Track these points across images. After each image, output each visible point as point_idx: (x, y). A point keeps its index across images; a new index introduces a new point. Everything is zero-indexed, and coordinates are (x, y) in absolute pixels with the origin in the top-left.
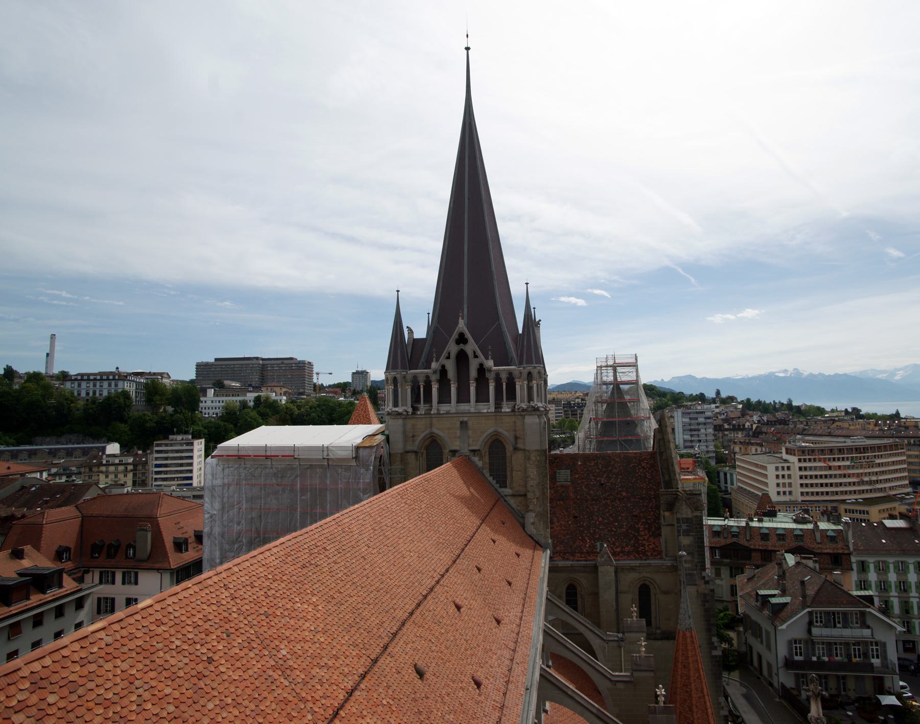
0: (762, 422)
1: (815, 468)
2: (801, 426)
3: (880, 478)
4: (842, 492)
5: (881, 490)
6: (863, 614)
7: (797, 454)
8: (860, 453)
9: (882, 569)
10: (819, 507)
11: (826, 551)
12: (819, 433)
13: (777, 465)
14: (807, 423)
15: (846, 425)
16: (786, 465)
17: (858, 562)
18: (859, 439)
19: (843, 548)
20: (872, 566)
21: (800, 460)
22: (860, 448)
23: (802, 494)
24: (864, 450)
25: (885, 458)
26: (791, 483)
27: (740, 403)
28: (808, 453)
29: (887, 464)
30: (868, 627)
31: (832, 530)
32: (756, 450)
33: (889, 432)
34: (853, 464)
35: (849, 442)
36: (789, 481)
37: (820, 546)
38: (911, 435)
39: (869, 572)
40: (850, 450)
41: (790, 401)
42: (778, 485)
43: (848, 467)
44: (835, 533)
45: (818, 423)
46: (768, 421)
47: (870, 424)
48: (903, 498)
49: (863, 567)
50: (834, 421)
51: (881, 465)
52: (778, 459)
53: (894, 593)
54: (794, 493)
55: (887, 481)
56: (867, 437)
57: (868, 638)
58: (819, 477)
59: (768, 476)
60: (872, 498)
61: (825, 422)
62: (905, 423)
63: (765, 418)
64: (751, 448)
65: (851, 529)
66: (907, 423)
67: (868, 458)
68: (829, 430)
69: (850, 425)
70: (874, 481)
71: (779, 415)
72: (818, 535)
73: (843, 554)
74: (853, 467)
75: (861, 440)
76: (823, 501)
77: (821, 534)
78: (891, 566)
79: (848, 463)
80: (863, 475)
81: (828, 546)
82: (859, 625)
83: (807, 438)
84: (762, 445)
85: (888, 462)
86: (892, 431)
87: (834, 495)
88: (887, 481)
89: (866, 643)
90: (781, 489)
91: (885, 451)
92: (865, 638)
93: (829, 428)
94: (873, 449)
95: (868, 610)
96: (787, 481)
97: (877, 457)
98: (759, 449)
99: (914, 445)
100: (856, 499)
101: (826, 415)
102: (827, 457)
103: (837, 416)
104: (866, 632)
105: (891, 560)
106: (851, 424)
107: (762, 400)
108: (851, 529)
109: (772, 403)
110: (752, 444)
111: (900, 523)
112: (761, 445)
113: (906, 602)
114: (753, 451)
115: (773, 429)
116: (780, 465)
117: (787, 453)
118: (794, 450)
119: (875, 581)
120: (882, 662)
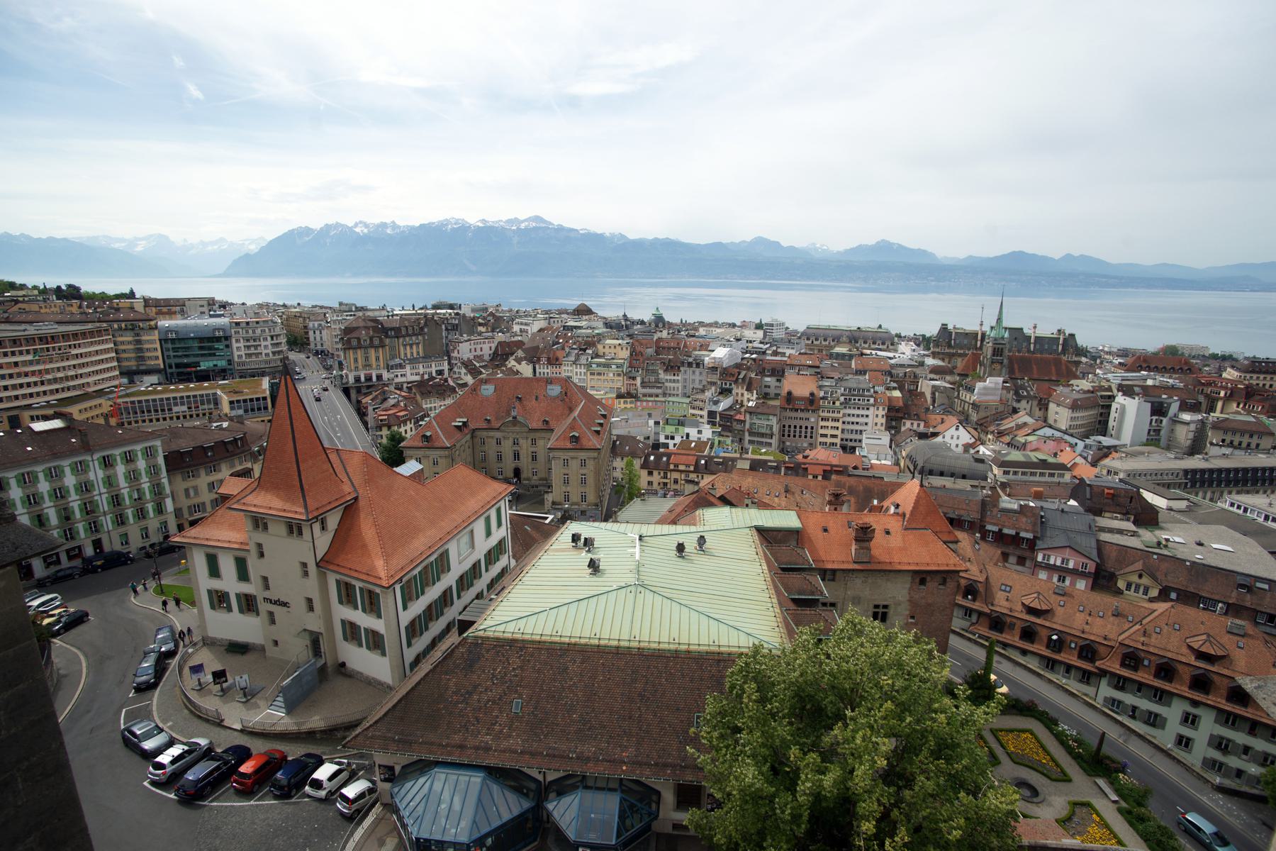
3: (80, 371)
4: (24, 396)
5: (74, 387)
8: (47, 344)
15: (35, 307)
22: (46, 337)
33: (94, 315)
34: (37, 358)
35: (31, 330)
38: (121, 319)
39: (10, 488)
40: (30, 340)
43: (31, 363)
48: (112, 392)
50: (17, 302)
51: (79, 356)
55: (89, 374)
56: (58, 323)
60: (71, 397)
67: (60, 349)
74: (38, 362)
75: (51, 327)
79: (30, 357)
86: (98, 315)
88: (89, 374)
91: (83, 339)
93: (5, 312)
94: (66, 338)
97: (73, 346)
99: (126, 329)
100: (48, 402)
102: (24, 348)
103: (24, 296)
105: (39, 469)
106: (43, 306)
119: (21, 498)
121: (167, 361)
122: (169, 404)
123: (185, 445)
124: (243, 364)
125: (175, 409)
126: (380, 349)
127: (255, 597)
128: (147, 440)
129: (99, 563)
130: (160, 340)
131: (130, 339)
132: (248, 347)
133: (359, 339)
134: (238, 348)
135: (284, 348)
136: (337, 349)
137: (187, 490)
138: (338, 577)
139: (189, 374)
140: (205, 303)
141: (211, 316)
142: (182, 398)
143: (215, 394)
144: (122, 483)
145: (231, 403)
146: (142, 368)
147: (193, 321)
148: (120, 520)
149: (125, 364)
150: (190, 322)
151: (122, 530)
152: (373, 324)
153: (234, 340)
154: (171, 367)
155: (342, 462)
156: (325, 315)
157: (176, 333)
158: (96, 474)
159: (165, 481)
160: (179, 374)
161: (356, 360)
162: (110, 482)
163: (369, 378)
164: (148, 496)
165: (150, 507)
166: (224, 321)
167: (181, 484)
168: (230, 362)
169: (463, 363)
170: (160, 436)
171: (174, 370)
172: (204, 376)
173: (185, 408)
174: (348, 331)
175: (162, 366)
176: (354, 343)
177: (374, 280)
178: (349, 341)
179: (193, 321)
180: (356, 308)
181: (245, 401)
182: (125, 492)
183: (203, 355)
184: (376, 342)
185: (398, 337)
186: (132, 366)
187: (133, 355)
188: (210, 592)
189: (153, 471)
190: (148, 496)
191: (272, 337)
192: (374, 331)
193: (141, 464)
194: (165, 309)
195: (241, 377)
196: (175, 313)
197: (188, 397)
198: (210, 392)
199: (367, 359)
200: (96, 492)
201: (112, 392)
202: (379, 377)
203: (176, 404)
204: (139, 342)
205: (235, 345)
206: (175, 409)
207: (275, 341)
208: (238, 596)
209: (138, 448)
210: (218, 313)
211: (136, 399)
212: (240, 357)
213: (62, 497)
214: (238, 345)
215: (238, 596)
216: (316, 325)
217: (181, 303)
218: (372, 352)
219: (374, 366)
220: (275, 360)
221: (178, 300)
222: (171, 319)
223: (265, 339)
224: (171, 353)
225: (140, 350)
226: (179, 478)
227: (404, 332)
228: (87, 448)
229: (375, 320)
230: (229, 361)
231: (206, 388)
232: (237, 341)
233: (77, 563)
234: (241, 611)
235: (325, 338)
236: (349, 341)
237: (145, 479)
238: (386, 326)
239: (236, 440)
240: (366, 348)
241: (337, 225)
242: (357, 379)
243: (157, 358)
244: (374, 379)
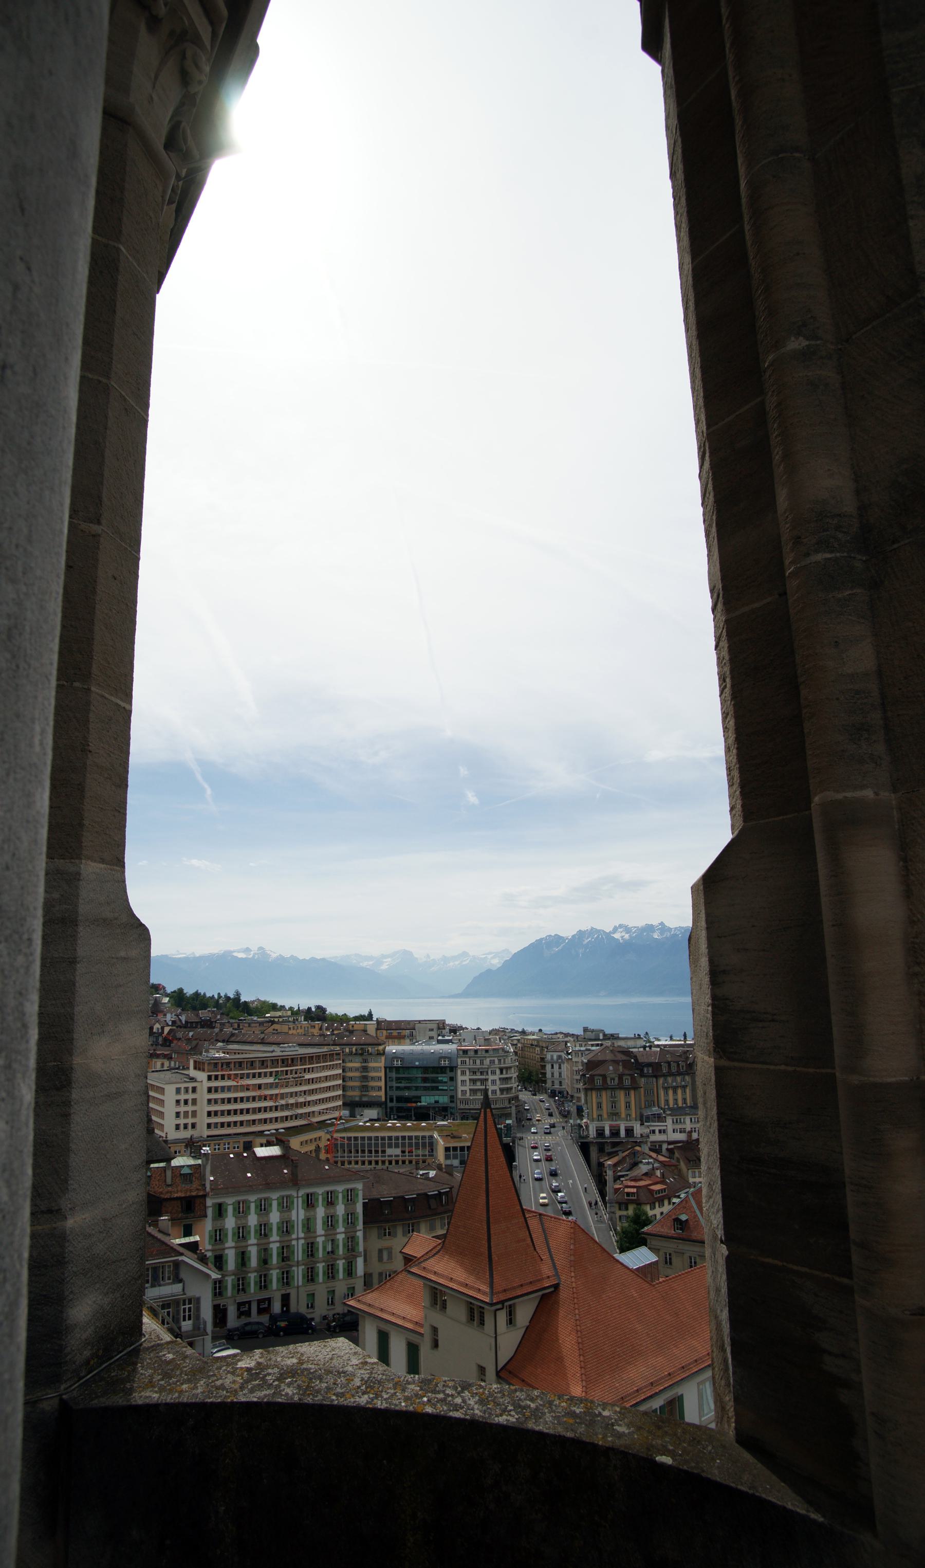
0: (179, 1023)
1: (229, 1089)
2: (228, 1030)
3: (309, 1098)
5: (301, 1116)
6: (177, 1265)
7: (206, 1068)
8: (287, 1067)
9: (241, 1210)
10: (229, 1144)
11: (176, 1195)
12: (249, 1040)
13: (178, 1086)
14: (239, 1026)
15: (285, 1028)
16: (191, 1085)
17: (214, 1205)
18: (290, 1047)
19: (198, 1189)
20: (230, 1209)
21: (209, 1078)
22: (288, 1059)
23: (209, 1126)
24: (292, 1062)
25: (317, 1072)
26: (196, 1111)
27: (167, 995)
28: (222, 1066)
29: (319, 1080)
30: (181, 1281)
31: (188, 1166)
32: (163, 1065)
34: (277, 1081)
35: (277, 1051)
36: (194, 1108)
37: (170, 1189)
38: (353, 1042)
39: (227, 1217)
40: (275, 1062)
41: (238, 994)
42: (178, 1115)
43: (271, 1086)
44: (191, 1170)
45: (252, 1025)
46: (186, 1022)
47: (314, 1027)
48: (332, 1124)
49: (220, 1211)
50: (273, 1022)
52: (183, 1076)
53: (253, 1240)
54: (198, 1126)
55: (316, 1102)
56: (300, 1045)
57: (177, 1295)
58: (232, 1101)
59: (165, 1102)
60: (297, 1127)
61: (261, 1024)
62: (353, 1026)
63: (183, 1018)
64: (156, 1062)
65: (210, 1162)
66: (355, 1026)
67: (296, 1073)
68: (262, 1036)
69: (290, 1028)
70: (292, 1104)
71: (204, 1014)
72: (169, 1173)
73: (197, 1197)
74: (276, 1086)
76: (235, 1134)
77: (172, 1173)
78: (253, 1206)
79: (271, 1080)
80: (279, 1097)
81: (179, 1188)
82: (171, 1281)
83: (231, 1047)
84: (171, 1058)
85: (320, 1077)
86: (334, 1036)
87: (250, 1126)
88: (316, 1102)
89: (177, 1303)
90: (182, 1121)
91: (317, 1063)
92: (174, 1296)
94: (303, 1061)
95: (180, 1258)
96: (190, 1108)
97: (307, 1070)
98: (167, 1063)
100: (277, 1130)
101: (267, 1015)
103: (280, 1017)
104: (177, 1288)
105: (253, 1198)
106: (291, 1027)
107: (202, 992)
108: (210, 1162)
109: (216, 997)
110: (158, 1056)
111: (275, 1151)
112: (170, 1058)
113: (266, 1250)
114: (158, 1067)
115: (191, 1034)
116: (183, 1086)
117: (195, 1068)
118: (204, 1063)
120: (194, 1325)
121: (389, 1093)
122: (383, 1145)
123: (386, 1193)
124: (467, 1101)
125: (389, 1151)
126: (632, 1093)
128: (349, 1181)
129: (282, 1324)
130: (385, 1068)
131: (357, 1065)
132: (473, 1081)
133: (604, 1077)
135: (514, 1084)
136: (578, 1090)
137: (380, 1251)
139: (409, 1109)
140: (435, 1026)
141: (439, 1042)
142: (397, 1138)
143: (431, 1137)
144: (320, 1230)
145: (447, 1149)
146: (365, 1099)
147: (420, 1048)
148: (311, 1276)
149: (350, 1093)
150: (417, 1048)
151: (311, 1288)
152: (624, 1058)
153: (459, 1072)
154: (391, 1100)
155: (544, 1230)
156: (566, 1044)
157: (402, 1060)
158: (298, 1214)
159: (360, 1234)
160: (399, 1109)
161: (599, 1106)
162: (308, 1225)
163: (615, 1133)
164: (341, 1251)
165: (341, 1264)
166: (451, 1048)
167: (377, 1243)
168: (452, 1098)
170: (363, 1177)
171: (394, 1104)
172: (423, 1115)
173: (398, 1151)
174: (591, 1065)
175: (383, 1099)
176: (598, 1082)
177: (635, 1000)
178: (592, 1079)
179: (420, 1048)
180: (605, 1035)
181: (462, 1149)
182: (320, 1240)
183: (426, 1088)
184: (627, 1082)
185: (656, 1077)
186: (355, 1096)
187: (357, 1084)
189: (350, 1219)
190: (341, 1251)
191: (501, 1070)
192: (624, 1067)
193: (340, 1209)
194: (395, 1033)
195: (462, 1119)
196: (404, 1037)
197: (404, 1138)
198: (427, 1134)
199: (614, 1104)
200: (294, 1236)
201: (332, 1124)
202: (629, 1131)
203: (390, 1146)
204: (365, 1069)
205: (460, 1078)
206: (389, 1151)
207: (504, 1076)
209: (340, 1188)
211: (352, 1135)
212: (464, 1092)
213: (266, 1235)
214: (464, 1078)
216: (555, 1057)
217: (411, 1026)
218: (621, 1095)
219: (623, 1116)
220: (502, 1099)
221: (408, 1022)
222: (399, 1044)
223: (494, 1073)
224: (395, 1084)
225: (365, 1078)
226: (374, 1233)
227: (665, 1071)
228: (295, 1182)
229: (627, 1053)
230: (452, 1097)
231: (423, 1129)
232: (463, 1073)
233: (265, 1319)
235: (564, 1075)
236: (592, 1079)
237: (341, 1229)
238: (641, 1060)
239: (440, 1194)
240: (613, 1089)
241: (593, 931)
242: (600, 1133)
243: (380, 1088)
244: (623, 1133)
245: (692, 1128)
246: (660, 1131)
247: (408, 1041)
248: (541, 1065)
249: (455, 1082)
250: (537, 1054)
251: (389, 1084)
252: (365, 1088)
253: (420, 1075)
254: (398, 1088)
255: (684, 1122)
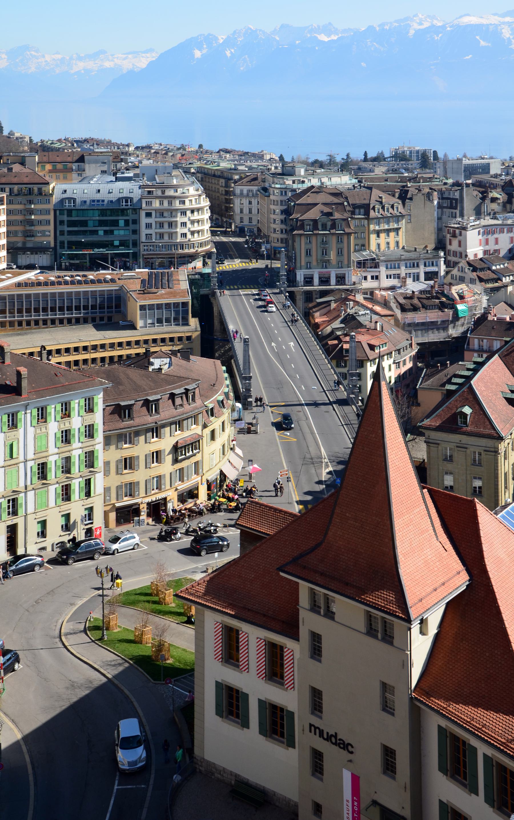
127: (291, 714)
130: (55, 211)
131: (20, 207)
134: (149, 226)
138: (444, 723)
153: (143, 214)
154: (62, 246)
161: (308, 253)
163: (325, 280)
169: (469, 264)
186: (17, 242)
188: (219, 685)
205: (144, 220)
208: (261, 702)
210: (126, 175)
214: (149, 220)
215: (261, 702)
216: (245, 192)
224: (66, 228)
232: (148, 215)
234: (262, 731)
245: (406, 274)
246: (372, 278)
247: (74, 175)
248: (225, 198)
249: (138, 225)
250: (222, 186)
251: (59, 228)
252: (29, 234)
253: (97, 218)
254: (70, 233)
255: (399, 268)
